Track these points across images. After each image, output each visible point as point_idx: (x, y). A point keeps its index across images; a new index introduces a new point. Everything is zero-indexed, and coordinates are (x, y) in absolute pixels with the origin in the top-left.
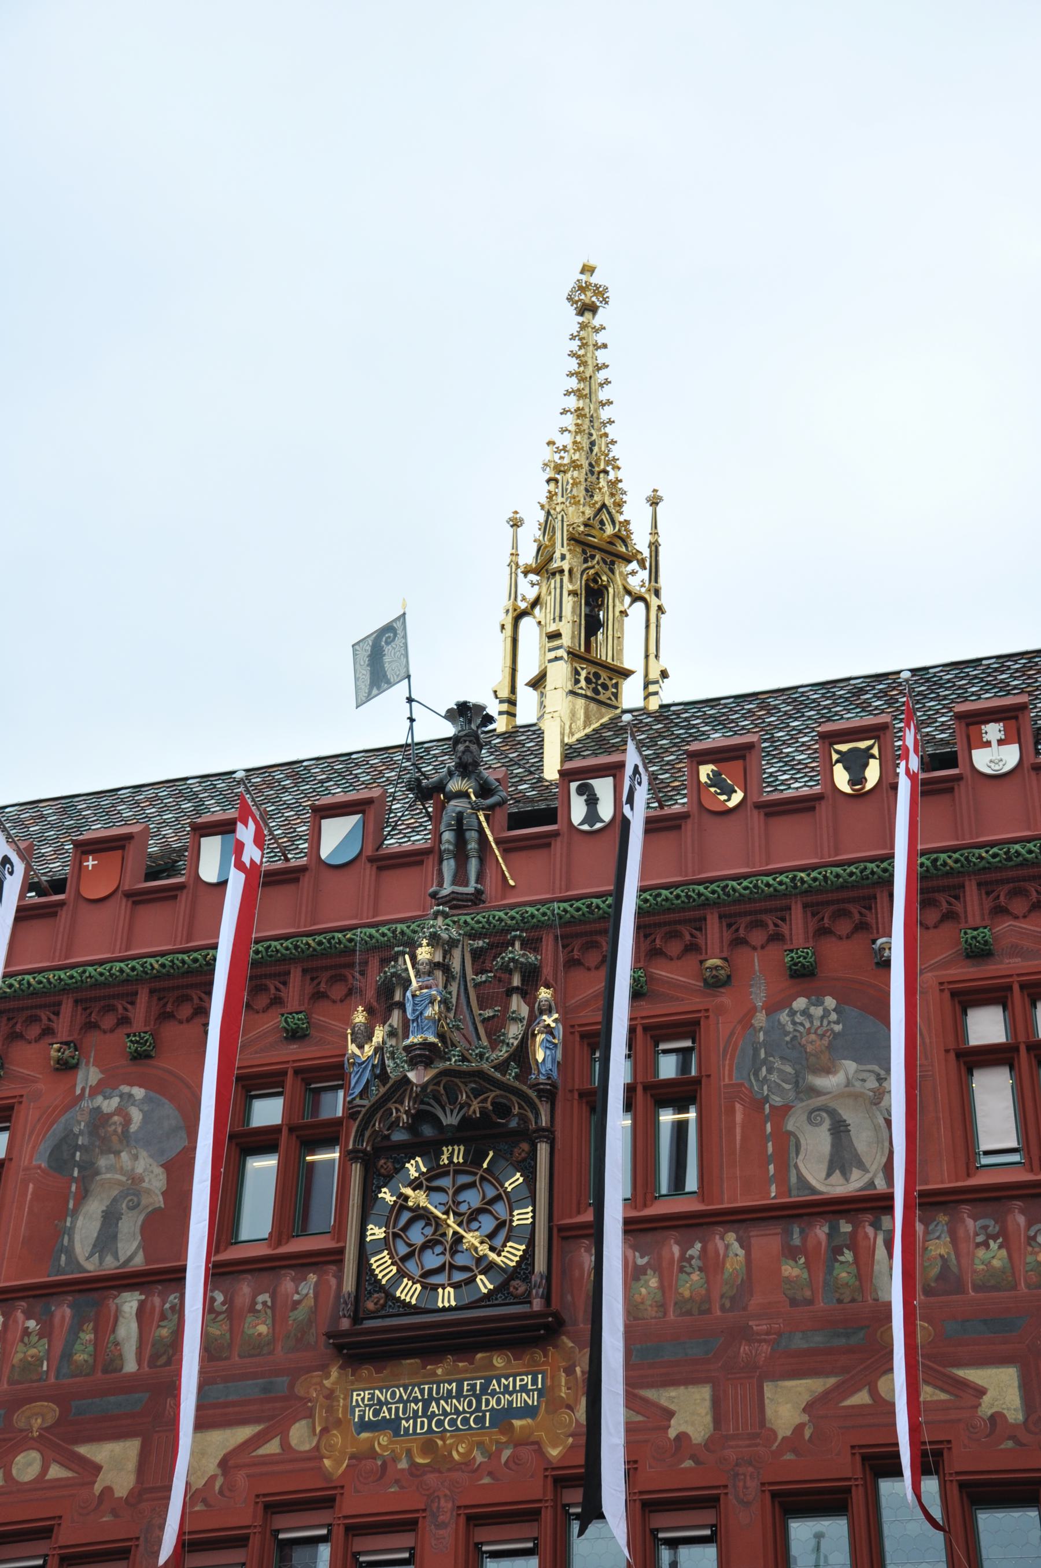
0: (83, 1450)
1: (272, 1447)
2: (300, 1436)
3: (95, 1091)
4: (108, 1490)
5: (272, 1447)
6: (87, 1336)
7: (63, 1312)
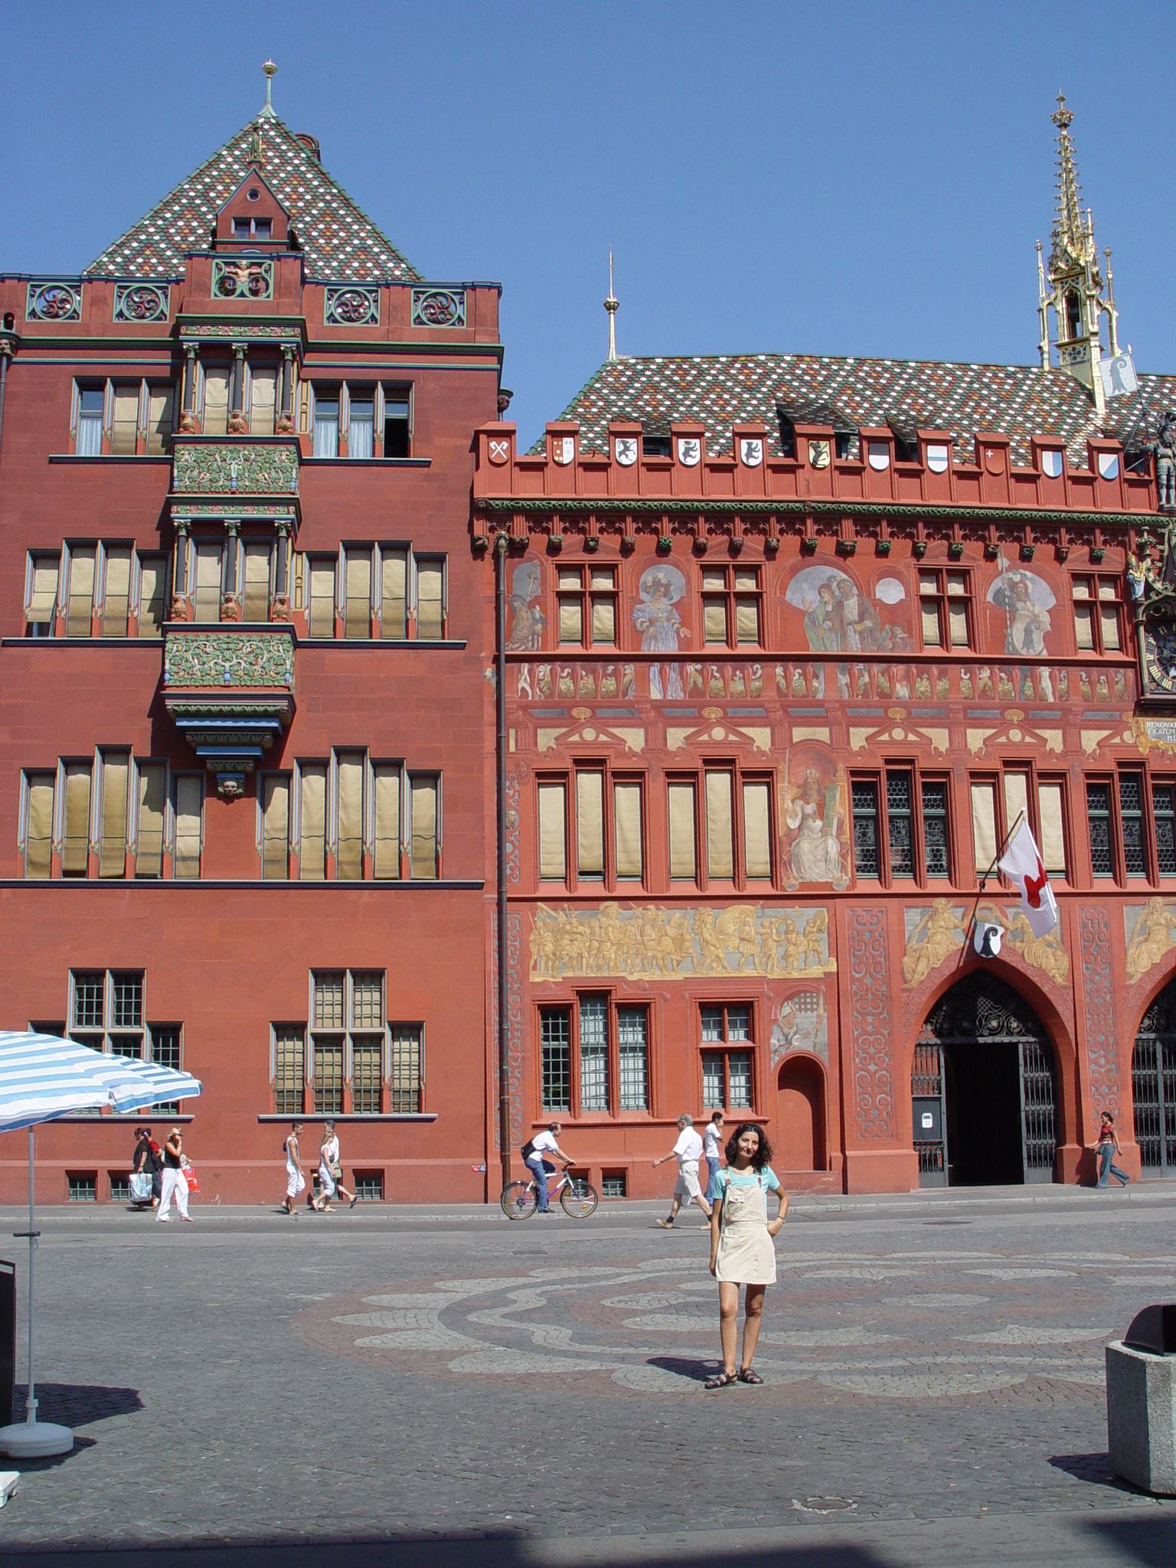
0: (1038, 731)
1: (1117, 740)
2: (1128, 737)
3: (1008, 569)
4: (1052, 750)
5: (1117, 740)
6: (1029, 684)
7: (1017, 670)
